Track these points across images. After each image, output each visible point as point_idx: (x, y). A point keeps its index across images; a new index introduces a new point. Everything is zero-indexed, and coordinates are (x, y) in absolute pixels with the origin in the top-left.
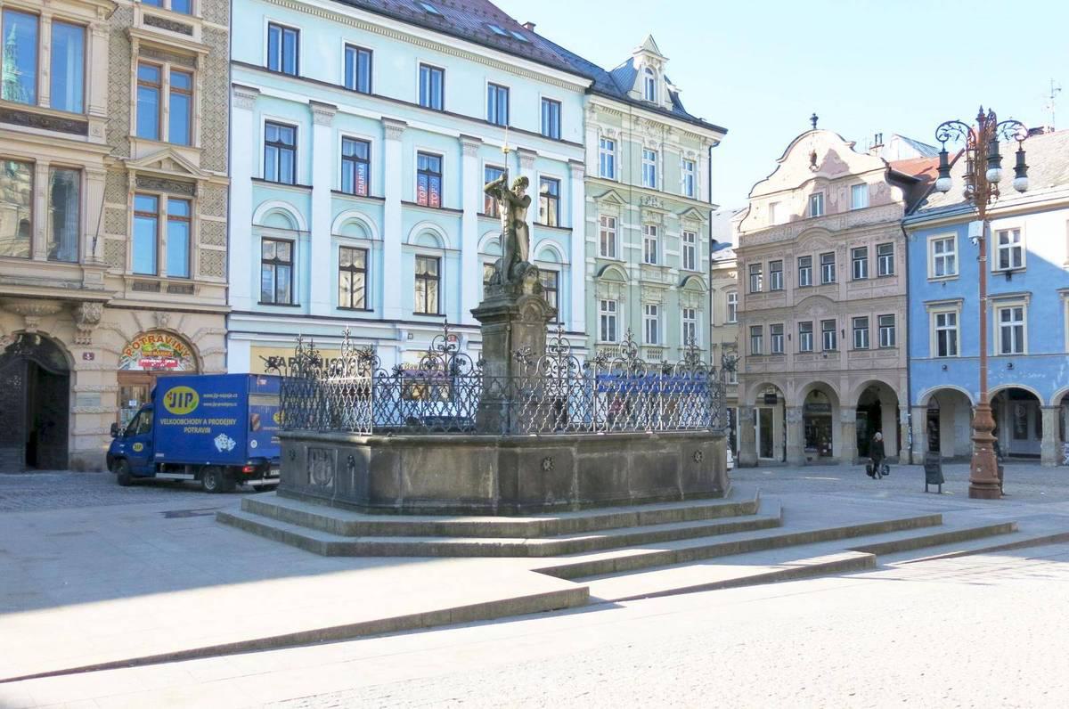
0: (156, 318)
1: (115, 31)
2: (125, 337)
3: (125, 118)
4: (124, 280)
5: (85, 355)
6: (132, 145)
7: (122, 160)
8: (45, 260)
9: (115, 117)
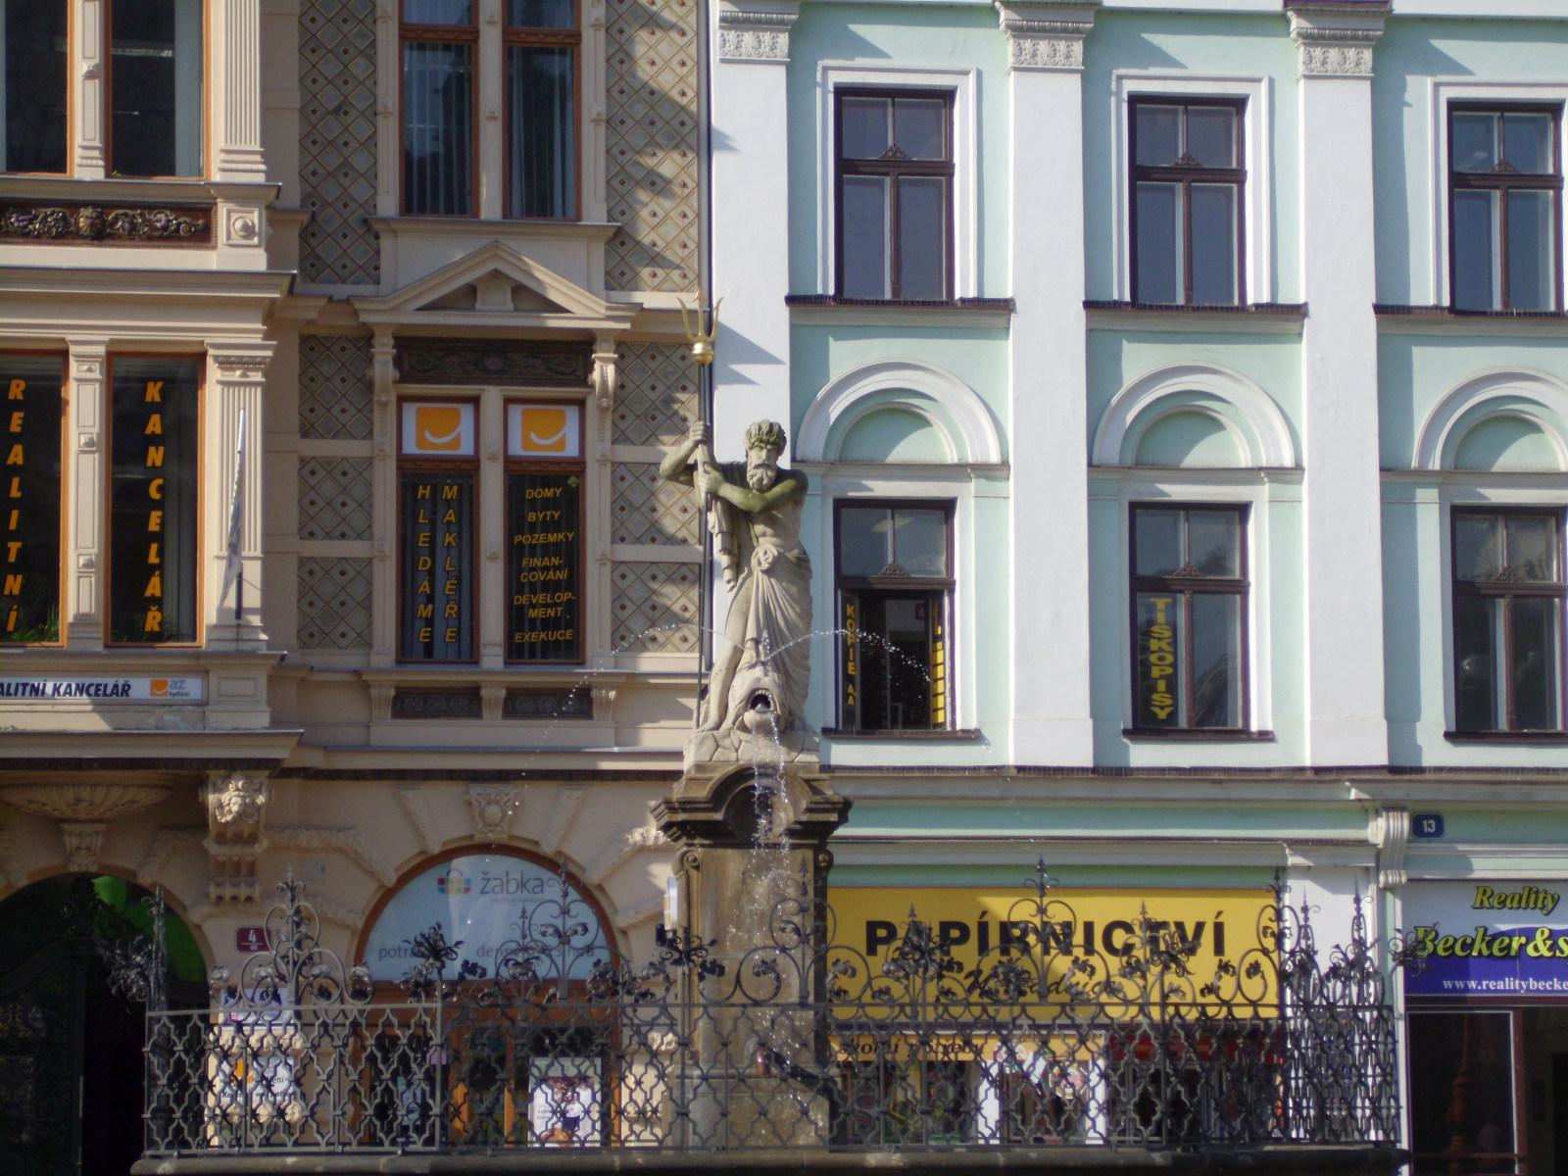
0: (470, 804)
2: (372, 874)
3: (360, 162)
4: (366, 686)
5: (242, 935)
6: (386, 244)
7: (348, 301)
8: (99, 647)
9: (333, 161)
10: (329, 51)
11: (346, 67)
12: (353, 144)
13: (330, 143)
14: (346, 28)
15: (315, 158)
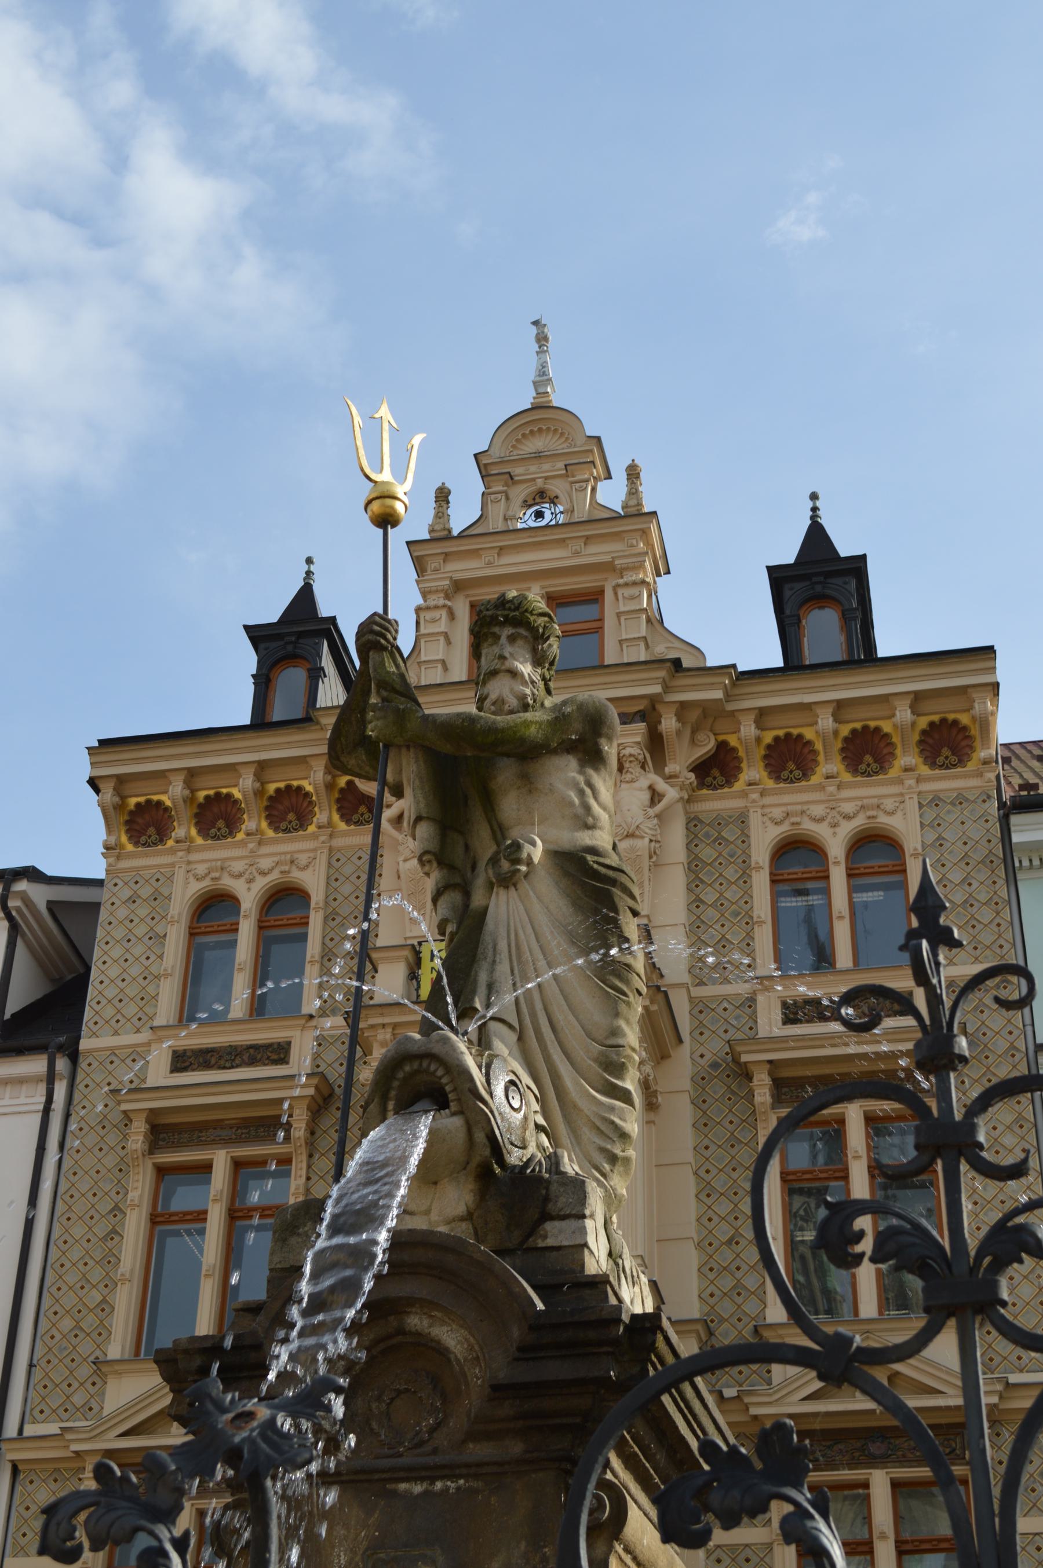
1: (715, 1065)
7: (738, 1398)
10: (722, 1194)
11: (736, 1205)
12: (744, 1268)
13: (725, 1268)
14: (735, 1175)
15: (712, 1282)
